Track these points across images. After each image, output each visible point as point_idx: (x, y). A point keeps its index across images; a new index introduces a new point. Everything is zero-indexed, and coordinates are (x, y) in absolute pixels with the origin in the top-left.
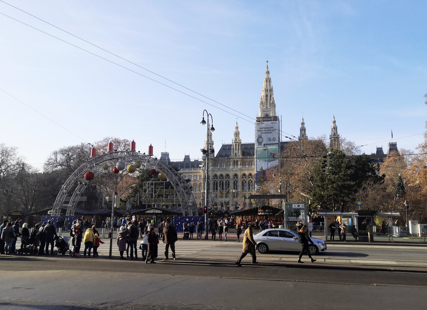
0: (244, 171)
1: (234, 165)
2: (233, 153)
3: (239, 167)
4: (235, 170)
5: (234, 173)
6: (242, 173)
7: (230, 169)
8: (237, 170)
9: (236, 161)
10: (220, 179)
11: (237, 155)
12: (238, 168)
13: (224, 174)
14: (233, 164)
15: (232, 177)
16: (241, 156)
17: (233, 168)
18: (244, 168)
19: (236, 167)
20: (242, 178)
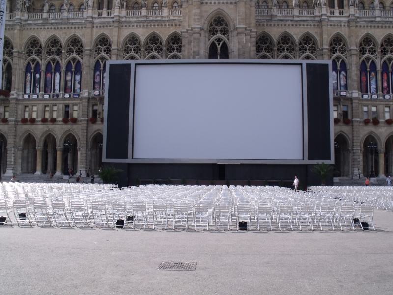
0: (133, 26)
1: (100, 7)
3: (117, 13)
4: (101, 23)
5: (97, 33)
6: (126, 32)
7: (84, 21)
8: (108, 23)
10: (49, 55)
12: (112, 16)
13: (63, 37)
14: (96, 5)
15: (89, 48)
17: (96, 16)
18: (134, 19)
19: (104, 15)
20: (125, 50)
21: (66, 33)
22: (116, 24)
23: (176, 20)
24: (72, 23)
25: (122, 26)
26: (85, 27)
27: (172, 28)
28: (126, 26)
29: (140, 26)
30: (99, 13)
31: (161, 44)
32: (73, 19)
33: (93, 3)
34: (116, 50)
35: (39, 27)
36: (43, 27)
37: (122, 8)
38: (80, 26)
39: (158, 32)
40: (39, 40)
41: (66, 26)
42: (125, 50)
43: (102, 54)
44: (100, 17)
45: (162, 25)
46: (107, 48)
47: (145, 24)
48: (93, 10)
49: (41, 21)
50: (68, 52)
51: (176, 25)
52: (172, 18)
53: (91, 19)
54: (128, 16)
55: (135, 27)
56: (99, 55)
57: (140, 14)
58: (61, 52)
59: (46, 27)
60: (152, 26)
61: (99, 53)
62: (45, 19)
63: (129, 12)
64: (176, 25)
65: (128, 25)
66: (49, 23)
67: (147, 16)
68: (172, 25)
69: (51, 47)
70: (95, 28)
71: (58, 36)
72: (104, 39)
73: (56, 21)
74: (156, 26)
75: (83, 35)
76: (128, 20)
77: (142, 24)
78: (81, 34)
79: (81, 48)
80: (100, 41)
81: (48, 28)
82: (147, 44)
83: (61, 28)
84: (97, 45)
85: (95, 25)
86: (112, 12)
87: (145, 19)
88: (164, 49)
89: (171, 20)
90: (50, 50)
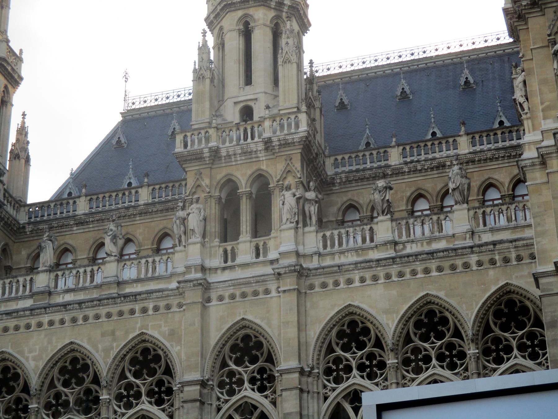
0: (349, 282)
2: (217, 113)
3: (288, 245)
4: (236, 283)
7: (174, 285)
8: (261, 280)
9: (244, 187)
11: (256, 117)
12: (272, 255)
14: (214, 227)
15: (196, 376)
16: (303, 117)
17: (216, 262)
18: (352, 258)
20: (328, 372)
21: (113, 333)
22: (290, 283)
23: (501, 242)
24: (135, 296)
25: (312, 287)
26: (180, 305)
27: (491, 273)
28: (324, 285)
29: (375, 278)
30: (225, 251)
31: (457, 334)
32: (138, 281)
33: (205, 219)
34: (296, 375)
35: (22, 323)
36: (33, 322)
37: (305, 225)
38: (162, 304)
39: (441, 294)
40: (17, 364)
41: (114, 310)
42: (328, 372)
43: (243, 393)
44: (229, 263)
45: (453, 267)
46: (262, 371)
47: (394, 270)
48: (203, 245)
49: (29, 303)
50: (119, 398)
51: (506, 260)
52: (487, 238)
53: (199, 275)
54: (329, 249)
55: (357, 284)
56: (234, 399)
57: (372, 240)
58: (97, 400)
59: (45, 319)
60: (419, 276)
61: (232, 393)
62: (42, 293)
63: (332, 236)
64: (506, 260)
65: (330, 281)
66: (57, 305)
67: (396, 243)
68: (493, 262)
69: (61, 388)
70: (214, 302)
71: (85, 345)
72: (246, 338)
73: (81, 296)
74: (434, 273)
75: (172, 334)
76: (328, 262)
77: (381, 272)
78: (165, 329)
79: (165, 378)
80: (234, 348)
81: (51, 323)
82: (408, 340)
83: (97, 317)
84: (224, 364)
85: (214, 295)
86: (271, 244)
87: (391, 253)
88: (472, 351)
89: (486, 244)
90: (58, 396)
